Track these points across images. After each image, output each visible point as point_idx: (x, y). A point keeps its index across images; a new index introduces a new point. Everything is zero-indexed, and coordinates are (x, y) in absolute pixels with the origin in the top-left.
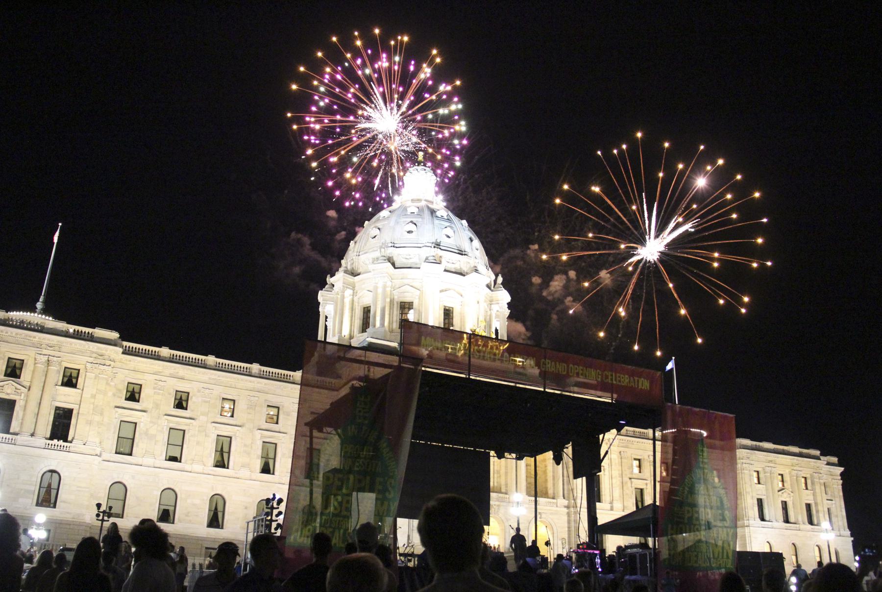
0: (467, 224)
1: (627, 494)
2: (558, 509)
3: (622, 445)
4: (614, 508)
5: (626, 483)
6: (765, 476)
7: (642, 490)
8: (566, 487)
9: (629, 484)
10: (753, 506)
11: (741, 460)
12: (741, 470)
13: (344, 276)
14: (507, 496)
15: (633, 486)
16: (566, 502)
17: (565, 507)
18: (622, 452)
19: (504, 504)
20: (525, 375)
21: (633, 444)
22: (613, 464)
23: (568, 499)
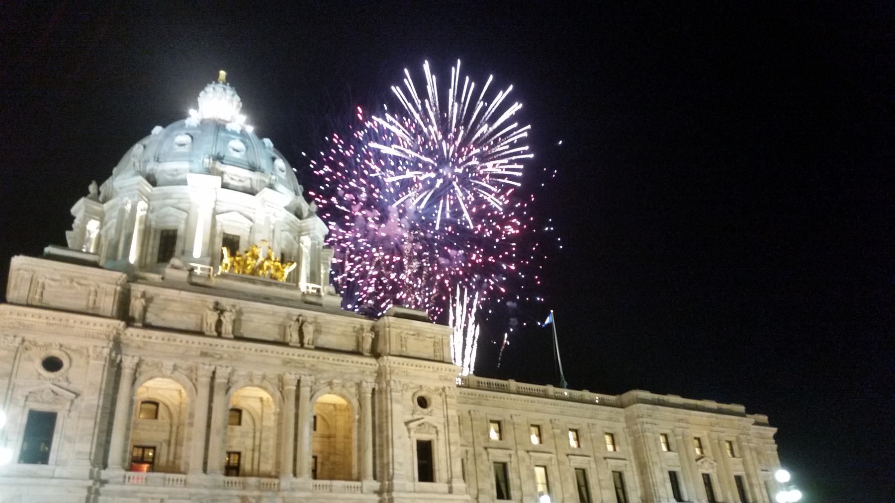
0: (272, 145)
1: (482, 471)
2: (363, 496)
3: (472, 401)
4: (454, 490)
5: (480, 455)
6: (676, 440)
7: (504, 465)
8: (378, 462)
9: (485, 457)
10: (665, 481)
11: (641, 419)
12: (642, 433)
13: (85, 201)
14: (276, 481)
15: (490, 458)
16: (376, 485)
17: (375, 492)
18: (472, 412)
19: (270, 494)
20: (321, 305)
21: (487, 400)
22: (451, 423)
23: (382, 481)
